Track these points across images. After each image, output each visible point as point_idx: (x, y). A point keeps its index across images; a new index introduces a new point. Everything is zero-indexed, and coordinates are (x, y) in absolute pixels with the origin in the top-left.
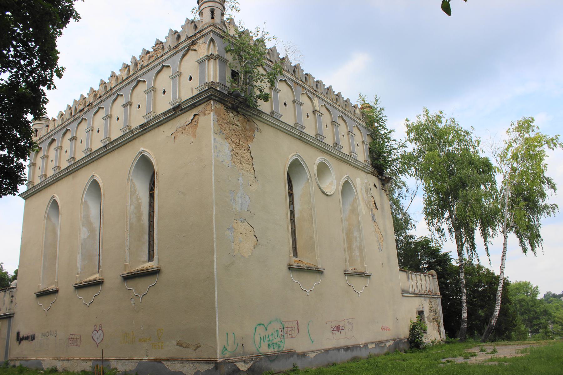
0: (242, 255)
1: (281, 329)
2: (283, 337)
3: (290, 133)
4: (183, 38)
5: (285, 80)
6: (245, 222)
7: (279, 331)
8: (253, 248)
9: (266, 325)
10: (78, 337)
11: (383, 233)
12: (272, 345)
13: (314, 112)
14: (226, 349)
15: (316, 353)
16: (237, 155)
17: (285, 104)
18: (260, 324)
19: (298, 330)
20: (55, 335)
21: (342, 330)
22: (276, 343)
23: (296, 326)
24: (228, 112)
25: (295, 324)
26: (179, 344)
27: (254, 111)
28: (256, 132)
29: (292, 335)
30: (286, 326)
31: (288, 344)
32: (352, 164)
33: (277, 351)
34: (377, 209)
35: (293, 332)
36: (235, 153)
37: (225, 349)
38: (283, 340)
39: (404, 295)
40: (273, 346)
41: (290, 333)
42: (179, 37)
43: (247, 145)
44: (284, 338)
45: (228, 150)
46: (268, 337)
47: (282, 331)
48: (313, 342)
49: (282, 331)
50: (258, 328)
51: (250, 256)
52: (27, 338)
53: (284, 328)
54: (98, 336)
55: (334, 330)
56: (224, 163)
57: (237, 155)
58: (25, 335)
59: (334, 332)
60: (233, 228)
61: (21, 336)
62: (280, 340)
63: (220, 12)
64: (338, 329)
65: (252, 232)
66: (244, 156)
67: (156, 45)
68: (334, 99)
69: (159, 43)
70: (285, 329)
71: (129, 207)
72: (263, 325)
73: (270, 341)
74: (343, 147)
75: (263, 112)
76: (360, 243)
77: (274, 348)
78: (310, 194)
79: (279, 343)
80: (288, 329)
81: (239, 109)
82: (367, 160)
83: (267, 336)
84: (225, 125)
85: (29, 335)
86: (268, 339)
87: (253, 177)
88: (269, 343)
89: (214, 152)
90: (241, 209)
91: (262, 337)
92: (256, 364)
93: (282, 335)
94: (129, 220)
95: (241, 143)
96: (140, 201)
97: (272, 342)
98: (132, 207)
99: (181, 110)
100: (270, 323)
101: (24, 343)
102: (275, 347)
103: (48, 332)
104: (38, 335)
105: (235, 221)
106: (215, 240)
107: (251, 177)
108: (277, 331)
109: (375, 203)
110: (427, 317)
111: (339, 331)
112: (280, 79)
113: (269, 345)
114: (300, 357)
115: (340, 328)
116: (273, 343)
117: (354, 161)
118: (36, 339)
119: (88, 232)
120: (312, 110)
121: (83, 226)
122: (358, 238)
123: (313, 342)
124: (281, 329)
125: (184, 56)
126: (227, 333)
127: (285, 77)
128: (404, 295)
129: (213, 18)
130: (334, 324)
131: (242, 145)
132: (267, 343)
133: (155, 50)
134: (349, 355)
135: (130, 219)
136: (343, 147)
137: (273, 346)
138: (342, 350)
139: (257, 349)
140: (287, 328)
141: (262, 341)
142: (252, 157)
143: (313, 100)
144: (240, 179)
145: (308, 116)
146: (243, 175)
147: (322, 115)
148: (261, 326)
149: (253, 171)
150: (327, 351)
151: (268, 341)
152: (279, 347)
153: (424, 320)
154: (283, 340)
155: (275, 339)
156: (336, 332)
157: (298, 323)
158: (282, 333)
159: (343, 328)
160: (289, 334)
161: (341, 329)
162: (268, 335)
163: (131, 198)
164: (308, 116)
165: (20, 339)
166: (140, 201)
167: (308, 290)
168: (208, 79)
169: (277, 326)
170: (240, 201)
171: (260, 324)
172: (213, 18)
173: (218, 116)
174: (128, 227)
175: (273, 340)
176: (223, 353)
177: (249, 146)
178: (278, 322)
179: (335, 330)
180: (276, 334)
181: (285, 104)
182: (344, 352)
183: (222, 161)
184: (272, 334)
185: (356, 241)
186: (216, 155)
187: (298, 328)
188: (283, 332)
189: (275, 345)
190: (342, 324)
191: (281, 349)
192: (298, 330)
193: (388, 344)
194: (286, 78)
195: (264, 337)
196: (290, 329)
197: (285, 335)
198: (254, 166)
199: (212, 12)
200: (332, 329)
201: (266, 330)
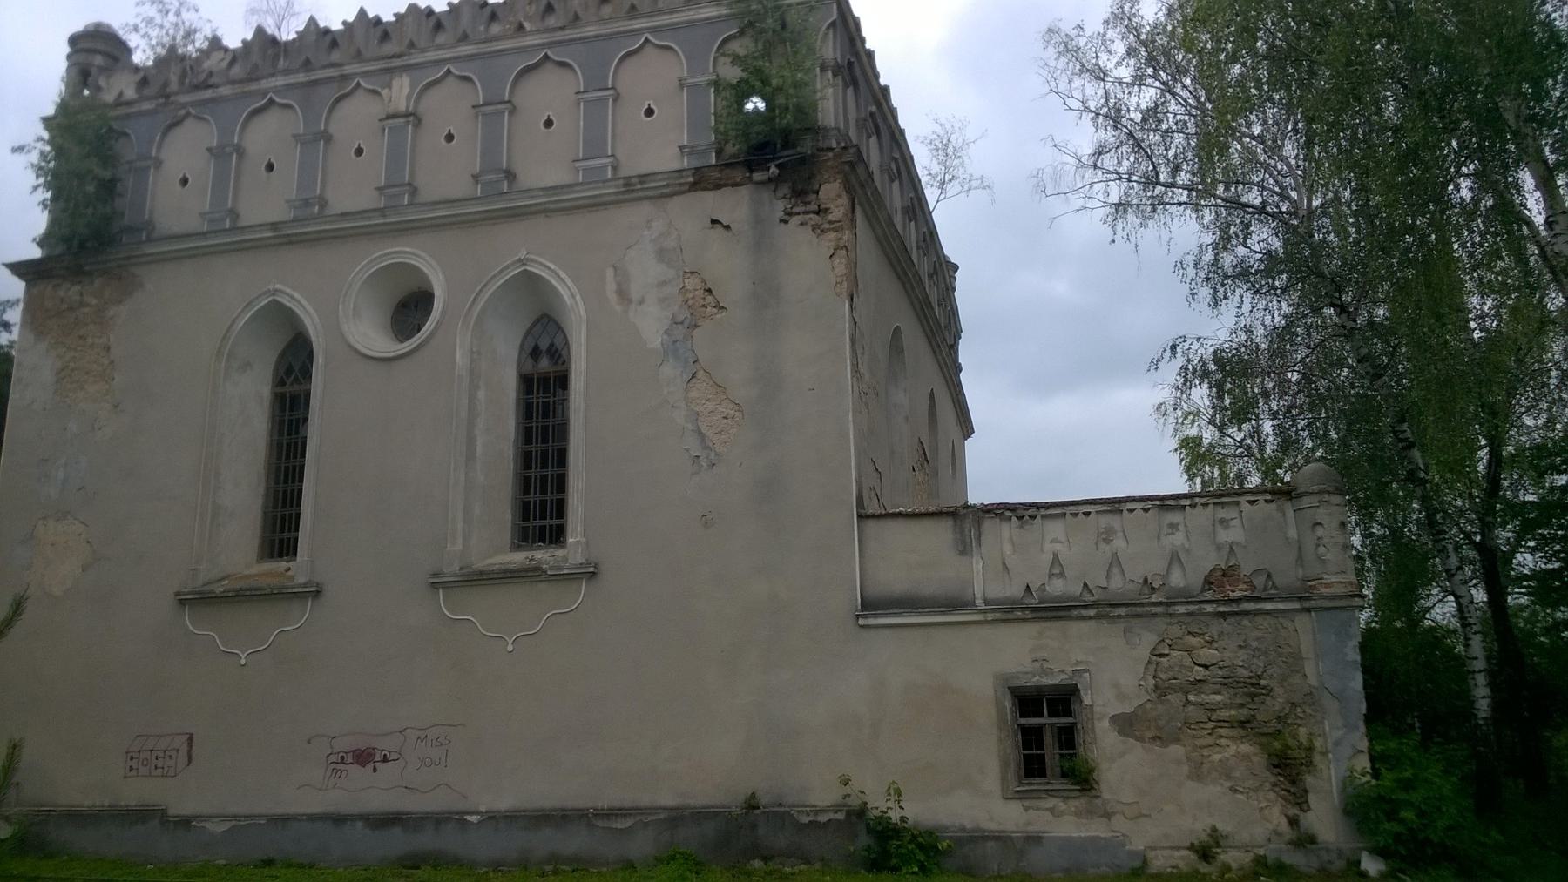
5: (271, 102)
15: (234, 823)
21: (385, 760)
23: (185, 747)
25: (180, 742)
29: (166, 769)
32: (552, 206)
33: (109, 806)
35: (172, 763)
41: (160, 765)
49: (132, 758)
59: (342, 766)
64: (363, 757)
81: (87, 268)
105: (41, 522)
111: (371, 766)
127: (265, 95)
128: (861, 622)
130: (344, 744)
134: (397, 842)
138: (360, 824)
150: (286, 819)
156: (355, 770)
157: (191, 739)
160: (156, 768)
167: (243, 653)
170: (61, 475)
200: (333, 758)
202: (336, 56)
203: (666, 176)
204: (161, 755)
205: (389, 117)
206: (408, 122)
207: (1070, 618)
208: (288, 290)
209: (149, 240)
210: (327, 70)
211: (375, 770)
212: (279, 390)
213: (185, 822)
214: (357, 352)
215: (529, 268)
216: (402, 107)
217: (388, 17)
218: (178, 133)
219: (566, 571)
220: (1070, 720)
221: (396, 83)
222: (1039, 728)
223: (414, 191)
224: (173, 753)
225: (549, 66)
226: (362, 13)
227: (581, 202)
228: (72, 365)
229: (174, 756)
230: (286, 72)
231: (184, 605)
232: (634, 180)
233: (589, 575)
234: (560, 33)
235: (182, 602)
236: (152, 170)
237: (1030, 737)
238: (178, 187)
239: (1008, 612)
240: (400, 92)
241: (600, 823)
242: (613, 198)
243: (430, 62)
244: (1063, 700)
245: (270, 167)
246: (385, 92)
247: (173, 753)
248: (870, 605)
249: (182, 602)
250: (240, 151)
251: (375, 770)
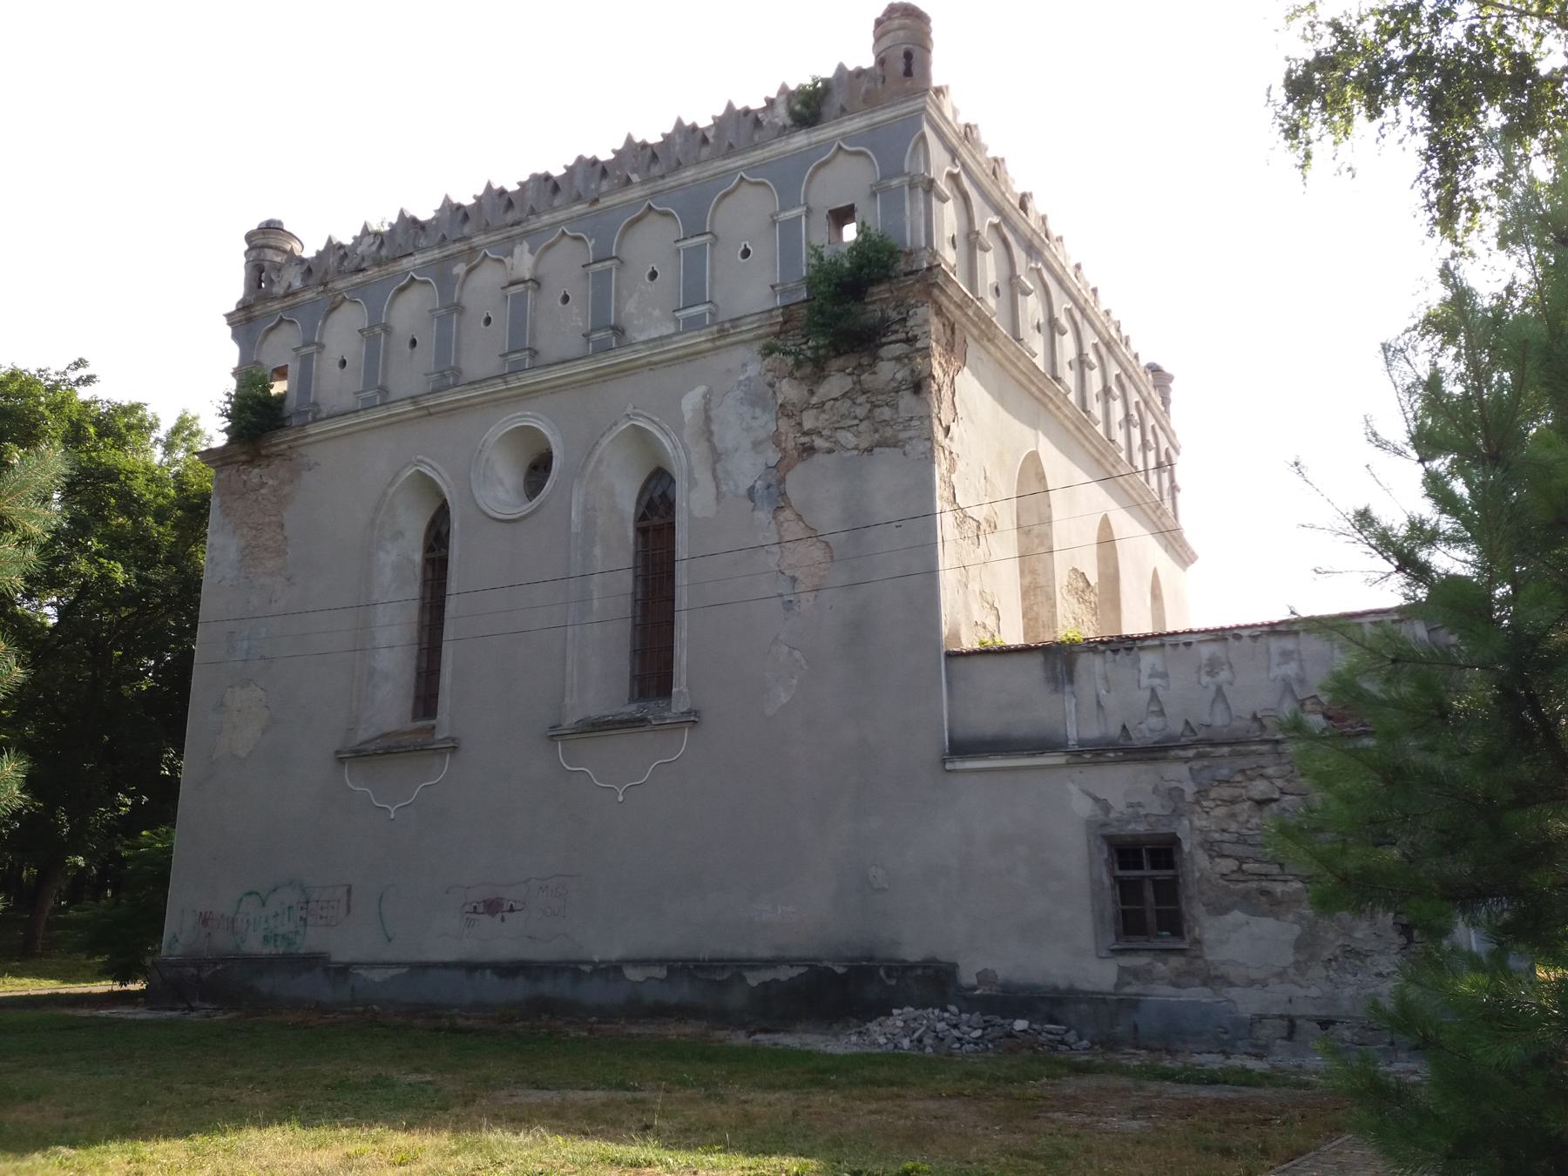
3: (394, 419)
18: (250, 894)
21: (512, 910)
22: (283, 937)
31: (312, 940)
39: (949, 766)
40: (276, 940)
41: (324, 915)
46: (266, 921)
47: (302, 908)
48: (390, 940)
49: (302, 908)
59: (474, 916)
64: (493, 907)
72: (257, 894)
77: (276, 946)
100: (274, 890)
102: (278, 943)
105: (229, 690)
111: (499, 916)
113: (265, 938)
116: (276, 935)
117: (656, 347)
123: (390, 940)
128: (949, 766)
134: (520, 989)
137: (276, 940)
138: (488, 972)
150: (425, 967)
151: (265, 929)
152: (290, 944)
156: (485, 918)
157: (349, 892)
161: (506, 907)
171: (250, 894)
175: (276, 927)
184: (276, 915)
187: (349, 901)
189: (279, 939)
191: (293, 950)
193: (754, 979)
194: (411, 273)
196: (325, 905)
197: (309, 918)
200: (469, 908)
201: (264, 905)
202: (467, 230)
203: (757, 317)
204: (325, 905)
205: (513, 284)
206: (527, 289)
207: (1165, 759)
208: (427, 460)
209: (315, 420)
210: (458, 244)
211: (503, 919)
212: (430, 555)
213: (344, 970)
214: (485, 514)
215: (635, 423)
216: (527, 276)
217: (512, 187)
218: (337, 316)
219: (668, 721)
220: (1171, 872)
221: (517, 250)
222: (1139, 881)
223: (534, 353)
225: (652, 217)
226: (489, 186)
227: (680, 353)
228: (254, 543)
230: (423, 250)
231: (344, 763)
232: (727, 325)
233: (691, 724)
234: (661, 182)
235: (341, 761)
236: (315, 356)
237: (1127, 891)
238: (338, 369)
239: (1096, 752)
240: (523, 261)
242: (709, 345)
243: (546, 226)
244: (1164, 851)
245: (414, 343)
246: (506, 261)
248: (961, 748)
249: (341, 761)
250: (387, 329)
251: (503, 919)
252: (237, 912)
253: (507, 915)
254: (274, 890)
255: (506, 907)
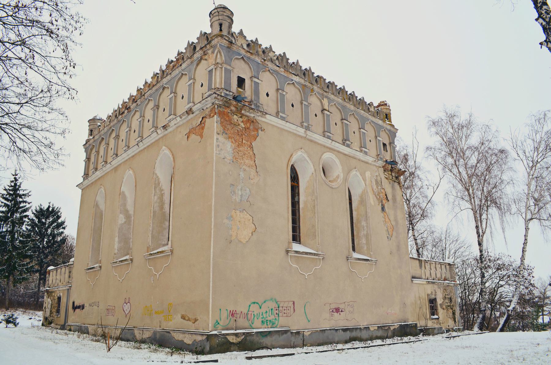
0: (239, 241)
1: (275, 308)
2: (277, 315)
4: (198, 48)
5: (293, 83)
6: (244, 211)
7: (274, 309)
8: (251, 234)
9: (260, 304)
10: (113, 308)
11: (393, 223)
12: (266, 322)
13: (323, 110)
14: (219, 323)
16: (240, 153)
17: (293, 106)
18: (254, 303)
19: (294, 310)
20: (98, 305)
21: (342, 311)
22: (270, 321)
24: (233, 114)
26: (183, 317)
27: (258, 112)
28: (260, 131)
29: (287, 314)
30: (281, 305)
34: (389, 201)
35: (289, 312)
36: (237, 151)
37: (217, 323)
38: (277, 318)
42: (195, 48)
43: (250, 143)
44: (279, 316)
45: (230, 148)
46: (262, 315)
47: (276, 310)
48: (309, 321)
49: (276, 310)
50: (252, 305)
51: (247, 241)
52: (79, 307)
53: (279, 307)
54: (127, 307)
55: (333, 312)
56: (225, 159)
57: (240, 153)
58: (78, 305)
59: (333, 313)
60: (232, 217)
61: (75, 305)
62: (275, 318)
63: (227, 24)
64: (337, 310)
65: (251, 220)
66: (247, 153)
67: (178, 55)
68: (347, 99)
69: (179, 54)
70: (280, 308)
71: (153, 197)
72: (257, 303)
73: (264, 319)
74: (352, 143)
75: (266, 113)
76: (367, 232)
77: (267, 325)
78: (314, 187)
79: (273, 321)
80: (284, 308)
82: (379, 155)
83: (261, 314)
84: (229, 127)
85: (81, 304)
86: (262, 317)
87: (255, 171)
88: (263, 319)
89: (216, 151)
90: (241, 200)
91: (256, 314)
92: (248, 338)
93: (276, 313)
94: (152, 209)
95: (244, 141)
96: (163, 192)
97: (266, 319)
98: (156, 197)
99: (193, 113)
100: (265, 302)
101: (77, 310)
102: (268, 323)
103: (93, 303)
104: (87, 305)
105: (234, 211)
106: (213, 227)
107: (253, 172)
108: (271, 309)
109: (386, 195)
110: (441, 305)
111: (339, 313)
112: (287, 83)
113: (262, 322)
114: (294, 334)
115: (339, 310)
116: (267, 320)
118: (85, 308)
119: (125, 218)
120: (320, 109)
121: (120, 213)
122: (365, 227)
123: (309, 321)
124: (275, 308)
125: (198, 65)
126: (220, 309)
129: (221, 30)
130: (334, 306)
131: (245, 143)
132: (260, 320)
133: (177, 60)
135: (154, 207)
136: (352, 143)
137: (267, 323)
139: (251, 325)
140: (282, 307)
141: (256, 318)
142: (254, 154)
143: (322, 100)
144: (241, 173)
145: (316, 115)
146: (245, 170)
147: (331, 114)
148: (256, 304)
149: (255, 167)
151: (262, 318)
152: (273, 324)
153: (436, 307)
154: (277, 318)
155: (270, 316)
156: (336, 314)
157: (294, 303)
158: (277, 312)
159: (343, 310)
160: (284, 313)
161: (340, 311)
162: (262, 313)
163: (155, 190)
164: (316, 115)
165: (75, 308)
166: (163, 192)
168: (215, 85)
169: (273, 305)
170: (240, 193)
171: (254, 303)
172: (221, 30)
173: (221, 119)
174: (152, 215)
175: (266, 317)
176: (215, 327)
177: (252, 144)
178: (273, 301)
179: (334, 311)
180: (271, 312)
181: (293, 106)
182: (343, 332)
183: (224, 158)
184: (266, 312)
185: (364, 230)
186: (218, 153)
187: (294, 308)
188: (278, 311)
189: (268, 322)
190: (341, 307)
192: (294, 310)
194: (294, 81)
195: (258, 315)
198: (256, 162)
199: (221, 25)
200: (331, 310)
211: (340, 314)
224: (289, 308)
229: (289, 309)
241: (383, 328)
247: (289, 308)
251: (340, 314)
252: (249, 311)
253: (341, 313)
254: (265, 302)
255: (340, 311)
